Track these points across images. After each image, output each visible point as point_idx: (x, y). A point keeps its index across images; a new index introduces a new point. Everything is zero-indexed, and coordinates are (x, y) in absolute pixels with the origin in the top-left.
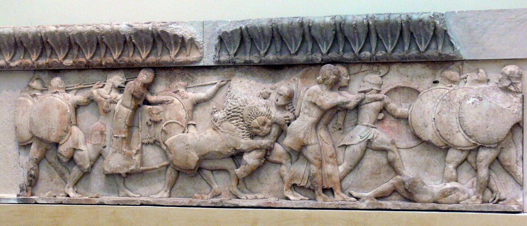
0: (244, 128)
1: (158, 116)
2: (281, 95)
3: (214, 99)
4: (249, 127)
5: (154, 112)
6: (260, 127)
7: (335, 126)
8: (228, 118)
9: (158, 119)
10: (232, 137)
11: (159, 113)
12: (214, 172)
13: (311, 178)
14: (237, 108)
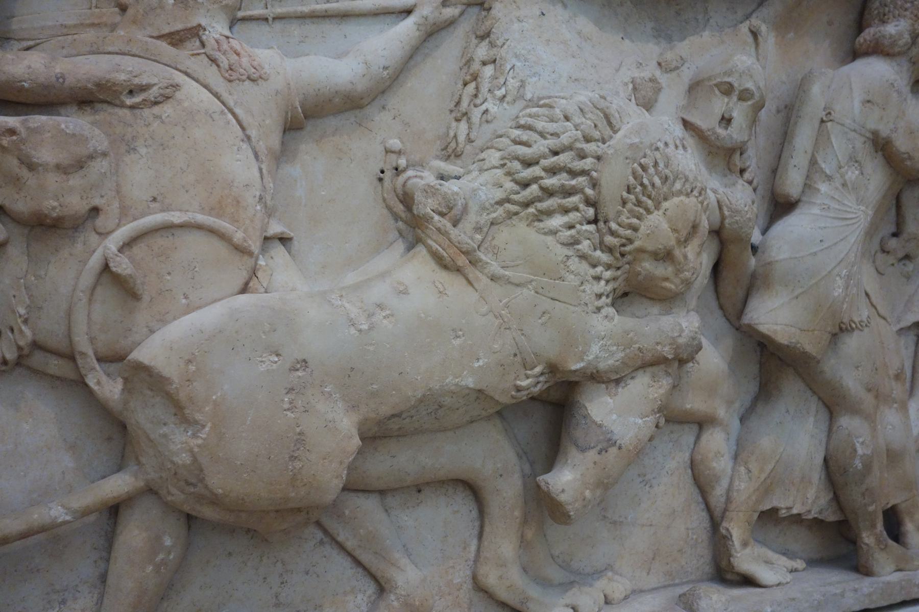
0: (598, 253)
1: (75, 181)
2: (745, 95)
3: (394, 101)
4: (622, 254)
5: (46, 155)
6: (677, 253)
7: (893, 243)
8: (526, 205)
9: (76, 204)
10: (547, 304)
11: (80, 165)
12: (390, 500)
13: (834, 472)
14: (570, 148)
